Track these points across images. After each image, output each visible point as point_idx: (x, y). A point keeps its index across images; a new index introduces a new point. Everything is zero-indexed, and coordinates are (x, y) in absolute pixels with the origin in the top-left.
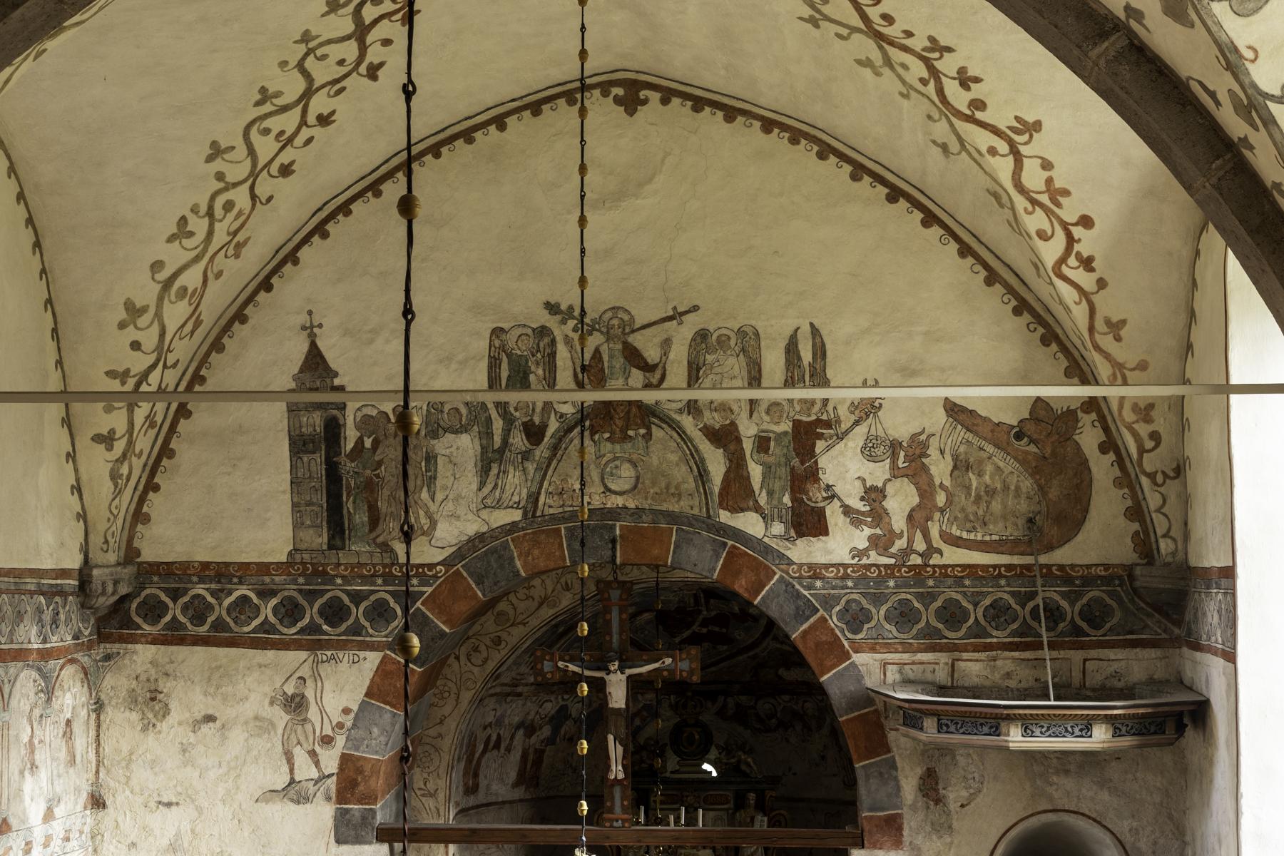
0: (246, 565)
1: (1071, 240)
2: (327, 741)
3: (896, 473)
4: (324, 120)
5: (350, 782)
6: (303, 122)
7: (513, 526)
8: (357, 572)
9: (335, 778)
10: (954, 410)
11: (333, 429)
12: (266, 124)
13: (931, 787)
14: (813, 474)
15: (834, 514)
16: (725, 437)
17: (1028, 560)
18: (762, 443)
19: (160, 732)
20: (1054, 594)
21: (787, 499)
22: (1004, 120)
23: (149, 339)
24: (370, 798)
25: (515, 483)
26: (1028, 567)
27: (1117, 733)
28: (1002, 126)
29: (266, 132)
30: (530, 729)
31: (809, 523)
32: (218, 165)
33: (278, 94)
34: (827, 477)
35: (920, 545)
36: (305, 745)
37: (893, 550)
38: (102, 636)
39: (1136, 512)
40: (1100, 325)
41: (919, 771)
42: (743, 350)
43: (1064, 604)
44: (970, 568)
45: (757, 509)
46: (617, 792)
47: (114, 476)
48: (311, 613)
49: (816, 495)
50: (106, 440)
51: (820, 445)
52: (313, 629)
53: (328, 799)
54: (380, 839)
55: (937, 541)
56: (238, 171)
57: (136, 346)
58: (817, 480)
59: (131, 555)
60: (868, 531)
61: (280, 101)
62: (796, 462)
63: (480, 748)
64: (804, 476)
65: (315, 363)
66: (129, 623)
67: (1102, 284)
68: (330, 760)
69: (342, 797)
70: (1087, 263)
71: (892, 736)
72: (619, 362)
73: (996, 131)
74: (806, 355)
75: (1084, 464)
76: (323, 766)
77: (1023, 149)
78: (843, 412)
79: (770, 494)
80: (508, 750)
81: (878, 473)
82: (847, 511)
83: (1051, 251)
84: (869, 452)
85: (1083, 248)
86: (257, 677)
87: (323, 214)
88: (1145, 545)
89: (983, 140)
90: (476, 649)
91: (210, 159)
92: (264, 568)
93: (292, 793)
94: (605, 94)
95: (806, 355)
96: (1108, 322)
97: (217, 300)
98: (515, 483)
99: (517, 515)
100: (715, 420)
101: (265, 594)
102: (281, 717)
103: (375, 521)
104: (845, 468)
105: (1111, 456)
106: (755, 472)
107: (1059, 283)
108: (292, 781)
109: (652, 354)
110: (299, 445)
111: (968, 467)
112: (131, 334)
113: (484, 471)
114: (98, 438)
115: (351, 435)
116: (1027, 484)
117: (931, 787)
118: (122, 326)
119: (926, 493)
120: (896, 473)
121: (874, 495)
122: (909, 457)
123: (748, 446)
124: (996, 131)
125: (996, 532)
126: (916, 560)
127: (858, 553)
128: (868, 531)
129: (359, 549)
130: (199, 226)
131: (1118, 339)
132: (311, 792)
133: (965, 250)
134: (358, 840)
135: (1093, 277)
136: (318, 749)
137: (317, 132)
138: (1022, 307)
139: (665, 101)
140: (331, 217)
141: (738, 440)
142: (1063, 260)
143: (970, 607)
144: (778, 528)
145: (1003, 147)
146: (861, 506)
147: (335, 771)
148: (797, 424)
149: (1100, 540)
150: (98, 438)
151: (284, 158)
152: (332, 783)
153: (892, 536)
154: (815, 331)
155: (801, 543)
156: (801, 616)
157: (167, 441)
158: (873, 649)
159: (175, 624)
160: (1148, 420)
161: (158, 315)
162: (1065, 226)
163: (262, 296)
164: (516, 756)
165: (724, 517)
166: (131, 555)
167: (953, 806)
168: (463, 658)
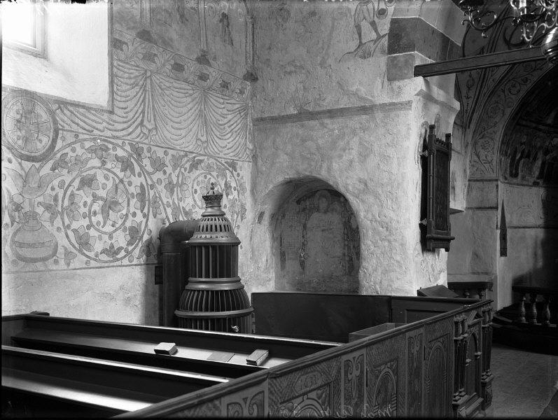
9: (387, 36)
19: (285, 29)
24: (411, 47)
30: (546, 152)
36: (368, 19)
53: (383, 52)
54: (416, 75)
63: (518, 156)
68: (385, 28)
69: (392, 49)
76: (379, 30)
80: (535, 159)
90: (514, 86)
93: (360, 53)
108: (361, 44)
132: (372, 49)
134: (402, 78)
136: (376, 20)
147: (387, 32)
152: (385, 41)
164: (539, 163)
168: (507, 92)
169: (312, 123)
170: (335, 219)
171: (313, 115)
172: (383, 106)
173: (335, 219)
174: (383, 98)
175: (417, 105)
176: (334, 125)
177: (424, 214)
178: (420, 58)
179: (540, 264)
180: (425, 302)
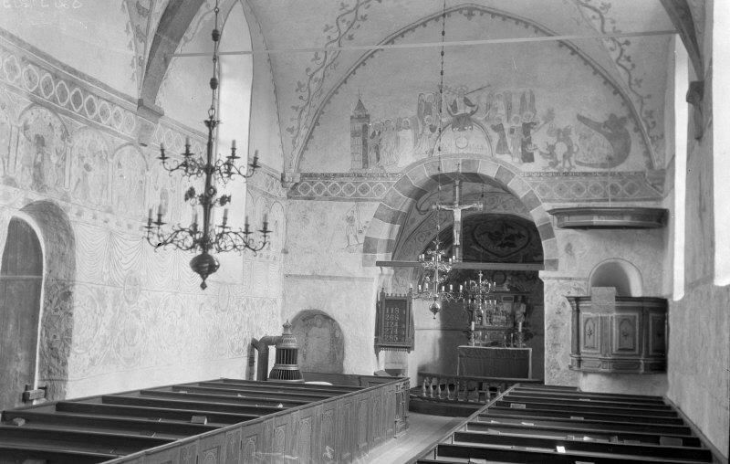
0: (335, 175)
1: (622, 51)
2: (361, 232)
3: (559, 140)
4: (364, 18)
5: (369, 246)
6: (356, 19)
7: (423, 161)
8: (371, 176)
10: (581, 118)
11: (365, 128)
12: (344, 17)
13: (569, 248)
14: (529, 141)
15: (536, 155)
16: (499, 128)
17: (606, 170)
18: (512, 131)
20: (616, 182)
21: (520, 150)
22: (598, 6)
23: (305, 95)
24: (375, 251)
25: (425, 147)
26: (607, 173)
27: (633, 219)
28: (598, 8)
29: (344, 21)
31: (528, 158)
32: (327, 34)
33: (348, 6)
34: (533, 142)
35: (567, 165)
37: (557, 167)
38: (289, 197)
39: (647, 153)
40: (633, 82)
41: (566, 243)
42: (506, 99)
43: (619, 185)
44: (586, 174)
45: (510, 153)
46: (457, 250)
47: (294, 142)
48: (357, 189)
49: (530, 149)
50: (291, 130)
51: (532, 131)
52: (356, 195)
54: (377, 265)
55: (573, 164)
56: (334, 37)
57: (301, 98)
58: (530, 143)
59: (299, 170)
60: (549, 161)
61: (349, 9)
62: (523, 137)
64: (526, 143)
65: (360, 106)
66: (297, 193)
67: (633, 66)
68: (362, 240)
69: (365, 251)
70: (628, 59)
71: (555, 231)
72: (463, 104)
73: (595, 10)
74: (528, 101)
75: (627, 136)
77: (604, 16)
78: (540, 118)
79: (514, 148)
81: (552, 141)
82: (541, 153)
83: (614, 55)
84: (549, 133)
85: (627, 53)
86: (336, 212)
87: (364, 58)
88: (650, 165)
89: (590, 13)
91: (325, 31)
92: (342, 175)
94: (461, 13)
95: (528, 101)
96: (636, 80)
97: (329, 84)
98: (425, 147)
99: (426, 156)
100: (496, 123)
101: (342, 183)
102: (346, 224)
103: (378, 159)
104: (540, 139)
105: (639, 133)
106: (509, 140)
107: (619, 68)
109: (474, 101)
110: (354, 134)
111: (585, 138)
112: (300, 93)
113: (416, 143)
114: (289, 130)
115: (371, 132)
116: (607, 143)
117: (569, 248)
118: (297, 90)
119: (570, 148)
120: (559, 140)
121: (552, 148)
122: (563, 135)
123: (506, 132)
124: (595, 10)
125: (595, 160)
126: (565, 170)
127: (545, 168)
128: (549, 161)
129: (371, 169)
130: (322, 55)
131: (640, 86)
133: (586, 62)
135: (630, 64)
137: (361, 23)
138: (607, 81)
139: (482, 15)
140: (367, 58)
141: (503, 129)
142: (619, 58)
143: (585, 187)
144: (516, 160)
145: (597, 15)
146: (545, 151)
148: (524, 124)
149: (635, 162)
150: (289, 130)
151: (350, 33)
152: (361, 247)
153: (557, 162)
154: (531, 92)
155: (526, 164)
156: (523, 190)
157: (311, 133)
158: (549, 201)
159: (312, 194)
160: (651, 117)
161: (308, 87)
162: (620, 45)
163: (344, 85)
165: (498, 156)
166: (299, 170)
167: (577, 257)
169: (320, 281)
170: (326, 331)
171: (320, 277)
172: (360, 279)
173: (326, 331)
174: (359, 274)
175: (376, 279)
176: (333, 284)
177: (377, 333)
178: (381, 257)
179: (438, 356)
180: (376, 380)
